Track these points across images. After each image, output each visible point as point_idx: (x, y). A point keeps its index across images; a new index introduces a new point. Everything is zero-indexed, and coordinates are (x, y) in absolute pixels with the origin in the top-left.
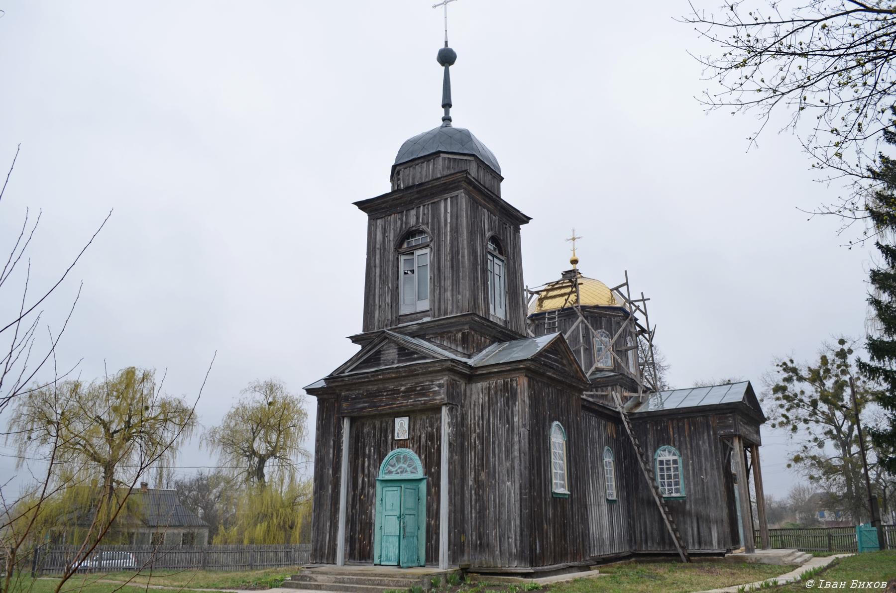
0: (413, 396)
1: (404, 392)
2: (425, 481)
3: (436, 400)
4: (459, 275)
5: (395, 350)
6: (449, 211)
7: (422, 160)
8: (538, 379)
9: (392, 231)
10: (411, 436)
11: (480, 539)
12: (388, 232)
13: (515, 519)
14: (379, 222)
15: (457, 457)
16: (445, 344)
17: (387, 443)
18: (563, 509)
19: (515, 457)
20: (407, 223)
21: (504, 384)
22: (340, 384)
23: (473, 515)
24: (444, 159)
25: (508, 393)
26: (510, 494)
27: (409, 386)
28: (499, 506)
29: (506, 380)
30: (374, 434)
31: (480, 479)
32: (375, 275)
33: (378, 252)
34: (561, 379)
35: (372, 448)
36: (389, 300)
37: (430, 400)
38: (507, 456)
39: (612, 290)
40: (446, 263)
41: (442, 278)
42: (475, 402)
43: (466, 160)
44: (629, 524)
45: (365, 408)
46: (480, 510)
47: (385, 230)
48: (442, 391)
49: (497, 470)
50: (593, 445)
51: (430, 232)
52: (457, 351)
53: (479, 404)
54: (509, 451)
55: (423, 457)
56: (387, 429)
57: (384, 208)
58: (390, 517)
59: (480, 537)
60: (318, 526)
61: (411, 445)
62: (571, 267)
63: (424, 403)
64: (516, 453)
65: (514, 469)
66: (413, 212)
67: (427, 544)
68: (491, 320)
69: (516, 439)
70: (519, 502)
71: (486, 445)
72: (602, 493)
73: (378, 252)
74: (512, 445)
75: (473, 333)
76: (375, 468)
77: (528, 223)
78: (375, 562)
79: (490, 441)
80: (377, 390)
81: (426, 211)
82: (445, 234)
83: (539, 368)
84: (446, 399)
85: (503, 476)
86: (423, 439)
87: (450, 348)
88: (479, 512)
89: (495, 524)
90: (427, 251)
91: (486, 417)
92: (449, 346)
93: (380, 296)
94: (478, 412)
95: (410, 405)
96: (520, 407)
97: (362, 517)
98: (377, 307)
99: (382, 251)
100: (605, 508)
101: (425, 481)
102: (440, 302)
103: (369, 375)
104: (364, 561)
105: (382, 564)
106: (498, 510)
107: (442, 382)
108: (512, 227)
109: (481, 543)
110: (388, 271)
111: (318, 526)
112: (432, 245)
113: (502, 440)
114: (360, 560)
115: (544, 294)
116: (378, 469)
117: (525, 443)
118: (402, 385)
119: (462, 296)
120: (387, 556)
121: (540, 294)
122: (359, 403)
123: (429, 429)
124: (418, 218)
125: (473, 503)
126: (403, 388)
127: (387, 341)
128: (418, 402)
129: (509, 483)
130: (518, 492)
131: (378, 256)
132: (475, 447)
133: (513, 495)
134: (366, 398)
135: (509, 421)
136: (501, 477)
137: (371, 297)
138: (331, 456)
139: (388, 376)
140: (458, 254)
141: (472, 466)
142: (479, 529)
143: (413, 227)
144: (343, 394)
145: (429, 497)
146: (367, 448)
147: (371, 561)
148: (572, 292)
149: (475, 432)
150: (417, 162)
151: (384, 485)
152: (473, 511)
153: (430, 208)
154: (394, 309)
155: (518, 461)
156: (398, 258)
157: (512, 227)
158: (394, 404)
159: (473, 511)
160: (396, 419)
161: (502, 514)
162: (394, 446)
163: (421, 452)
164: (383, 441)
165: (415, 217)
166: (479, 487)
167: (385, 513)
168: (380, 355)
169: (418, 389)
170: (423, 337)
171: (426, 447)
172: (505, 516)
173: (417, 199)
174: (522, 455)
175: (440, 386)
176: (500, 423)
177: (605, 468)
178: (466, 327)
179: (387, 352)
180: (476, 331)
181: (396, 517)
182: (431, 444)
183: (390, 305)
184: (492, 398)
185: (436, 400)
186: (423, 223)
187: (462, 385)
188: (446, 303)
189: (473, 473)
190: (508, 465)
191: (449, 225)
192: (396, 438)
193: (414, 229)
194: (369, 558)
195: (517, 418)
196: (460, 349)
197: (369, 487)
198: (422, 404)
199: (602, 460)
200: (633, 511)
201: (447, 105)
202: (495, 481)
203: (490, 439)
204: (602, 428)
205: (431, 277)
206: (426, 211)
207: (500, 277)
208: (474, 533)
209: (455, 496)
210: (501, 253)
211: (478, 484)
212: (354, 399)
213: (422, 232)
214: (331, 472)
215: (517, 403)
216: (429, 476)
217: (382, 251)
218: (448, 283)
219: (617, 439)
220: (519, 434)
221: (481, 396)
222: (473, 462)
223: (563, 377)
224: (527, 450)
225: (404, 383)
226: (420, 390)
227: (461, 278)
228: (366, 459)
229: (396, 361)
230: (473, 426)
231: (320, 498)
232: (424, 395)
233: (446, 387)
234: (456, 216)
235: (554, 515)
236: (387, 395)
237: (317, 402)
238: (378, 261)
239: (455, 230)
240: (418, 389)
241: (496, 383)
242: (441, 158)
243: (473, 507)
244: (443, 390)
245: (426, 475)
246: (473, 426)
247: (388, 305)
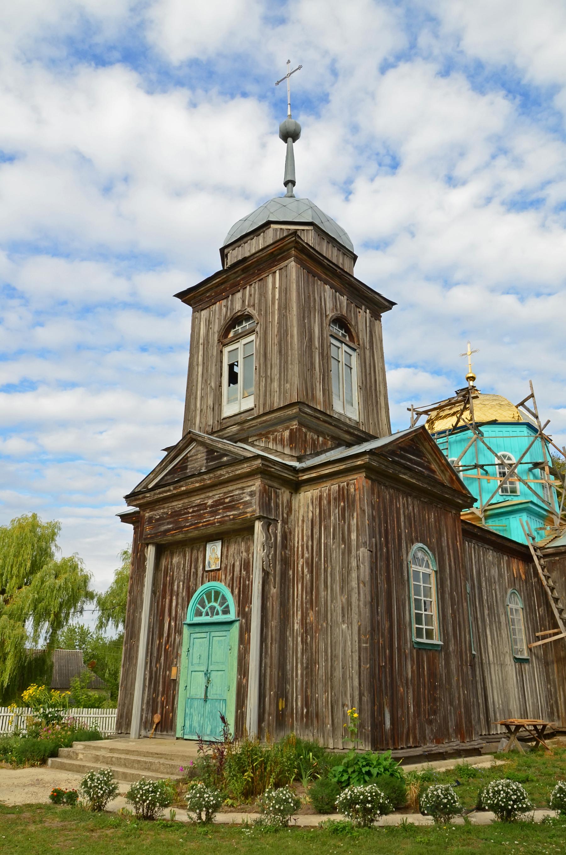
0: (221, 511)
1: (211, 506)
2: (237, 624)
3: (246, 513)
4: (287, 360)
5: (203, 455)
6: (277, 285)
7: (252, 236)
8: (387, 484)
9: (217, 321)
10: (223, 566)
11: (307, 706)
12: (212, 323)
13: (352, 679)
14: (204, 313)
15: (275, 590)
16: (270, 446)
17: (197, 575)
18: (432, 664)
19: (352, 589)
20: (232, 309)
21: (339, 490)
23: (299, 672)
24: (276, 230)
25: (344, 502)
26: (345, 642)
27: (217, 498)
28: (331, 659)
29: (342, 485)
30: (184, 565)
31: (308, 621)
32: (197, 375)
33: (201, 347)
34: (425, 486)
35: (181, 583)
36: (210, 402)
37: (241, 513)
38: (342, 589)
39: (517, 407)
40: (273, 349)
41: (269, 366)
42: (303, 517)
43: (304, 230)
44: (549, 691)
45: (169, 530)
46: (307, 664)
47: (209, 323)
48: (253, 501)
49: (329, 608)
50: (491, 585)
51: (256, 314)
52: (284, 454)
53: (308, 520)
54: (345, 581)
55: (236, 591)
58: (197, 673)
59: (306, 703)
60: (126, 684)
61: (223, 577)
62: (465, 385)
63: (233, 519)
64: (354, 584)
65: (351, 605)
66: (239, 295)
67: (237, 712)
68: (328, 413)
69: (354, 564)
70: (357, 654)
71: (317, 573)
72: (507, 649)
73: (201, 347)
74: (349, 573)
75: (304, 430)
76: (183, 609)
77: (391, 309)
78: (177, 736)
79: (320, 569)
80: (183, 506)
81: (253, 292)
82: (273, 313)
83: (386, 466)
84: (258, 511)
85: (337, 617)
86: (237, 569)
87: (277, 451)
88: (307, 668)
89: (326, 685)
90: (252, 337)
91: (316, 536)
92: (275, 448)
93: (202, 397)
94: (307, 532)
95: (218, 522)
96: (359, 519)
97: (166, 673)
98: (198, 412)
99: (205, 346)
100: (511, 669)
101: (237, 624)
102: (265, 396)
104: (165, 733)
105: (186, 737)
106: (330, 664)
107: (253, 488)
108: (368, 311)
109: (307, 712)
110: (211, 367)
111: (126, 684)
112: (258, 329)
113: (336, 567)
114: (161, 731)
115: (433, 414)
116: (186, 609)
117: (365, 569)
118: (209, 497)
119: (291, 385)
120: (191, 726)
121: (429, 415)
122: (163, 524)
124: (243, 302)
125: (299, 655)
126: (210, 502)
127: (194, 444)
128: (226, 518)
129: (344, 626)
130: (356, 638)
131: (201, 353)
132: (303, 578)
133: (349, 643)
134: (170, 518)
135: (345, 540)
136: (334, 618)
137: (193, 401)
140: (287, 335)
141: (299, 603)
142: (306, 691)
143: (238, 311)
144: (147, 515)
145: (241, 646)
146: (176, 584)
147: (173, 733)
148: (465, 409)
149: (303, 557)
150: (245, 240)
151: (192, 630)
152: (299, 666)
153: (257, 288)
154: (216, 412)
155: (357, 595)
156: (221, 352)
157: (368, 311)
158: (200, 523)
159: (299, 666)
160: (207, 545)
161: (335, 670)
162: (205, 579)
163: (235, 585)
164: (194, 572)
165: (241, 301)
166: (306, 631)
167: (191, 669)
168: (187, 462)
169: (227, 500)
170: (244, 440)
171: (240, 577)
172: (338, 674)
173: (242, 279)
174: (361, 585)
175: (252, 494)
176: (334, 543)
177: (510, 617)
178: (295, 422)
179: (195, 457)
180: (309, 428)
181: (203, 673)
182: (246, 573)
183: (212, 407)
184: (324, 510)
185: (246, 513)
186: (249, 306)
187: (285, 495)
188: (272, 394)
189: (299, 613)
190: (344, 600)
191: (277, 302)
192: (207, 569)
193: (239, 314)
194: (172, 729)
195: (355, 534)
196: (287, 451)
197: (175, 633)
198: (230, 520)
199: (505, 607)
200: (553, 674)
202: (327, 623)
203: (321, 565)
204: (504, 565)
205: (256, 367)
206: (253, 292)
207: (351, 369)
208: (299, 697)
209: (271, 644)
210: (352, 339)
211: (306, 627)
212: (157, 520)
213: (249, 317)
215: (355, 515)
216: (243, 618)
217: (205, 346)
218: (276, 371)
219: (526, 581)
220: (358, 557)
221: (311, 508)
222: (300, 597)
223: (428, 484)
224: (367, 578)
226: (230, 502)
227: (289, 362)
228: (174, 598)
230: (300, 549)
231: (130, 649)
232: (232, 508)
233: (258, 495)
234: (285, 291)
235: (419, 673)
236: (193, 512)
237: (133, 531)
238: (200, 358)
239: (284, 307)
240: (227, 500)
241: (329, 490)
242: (271, 230)
243: (299, 660)
244: (256, 500)
245: (238, 616)
246: (300, 549)
247: (210, 408)
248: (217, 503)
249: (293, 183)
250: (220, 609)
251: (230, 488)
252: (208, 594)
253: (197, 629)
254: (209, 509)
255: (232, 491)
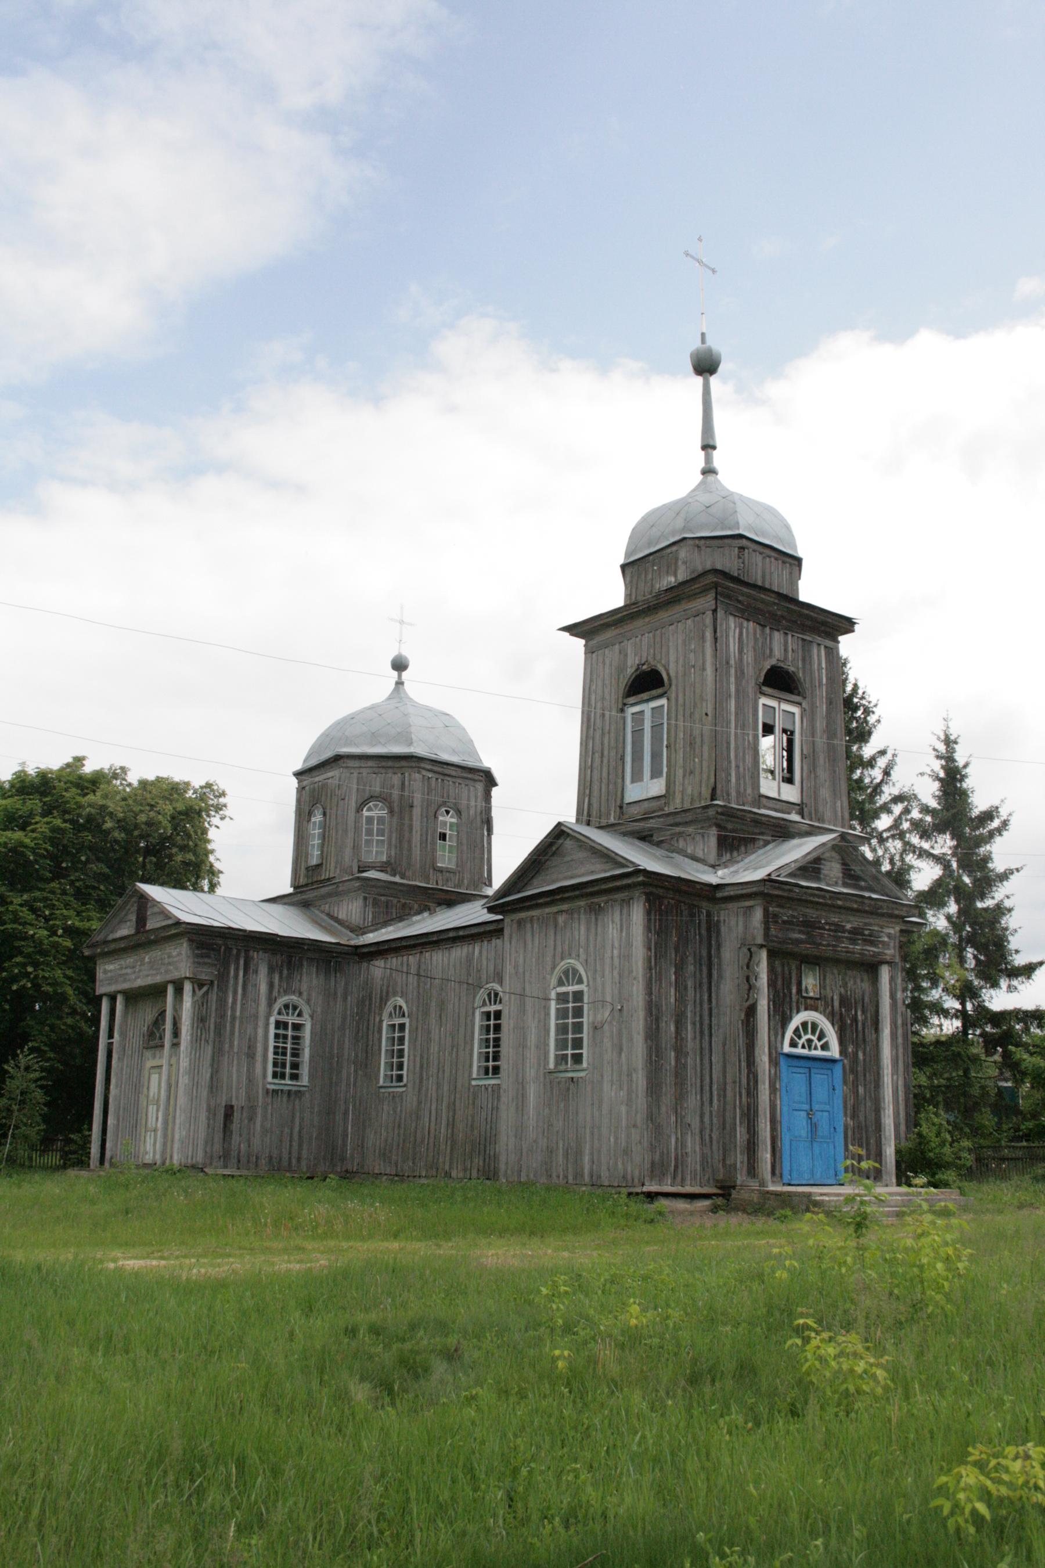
1: (850, 932)
22: (785, 894)
27: (855, 925)
33: (733, 671)
48: (892, 944)
56: (791, 978)
57: (739, 602)
63: (873, 956)
73: (733, 671)
86: (836, 1004)
103: (827, 895)
107: (892, 931)
118: (848, 922)
122: (793, 930)
123: (842, 990)
126: (848, 926)
131: (732, 679)
138: (672, 1000)
139: (848, 904)
151: (790, 1060)
175: (889, 936)
201: (708, 447)
212: (784, 922)
214: (673, 1028)
225: (852, 918)
229: (840, 882)
232: (872, 943)
248: (856, 932)
249: (714, 448)
250: (819, 1044)
251: (872, 921)
252: (804, 1025)
253: (796, 1062)
254: (846, 935)
255: (870, 924)
